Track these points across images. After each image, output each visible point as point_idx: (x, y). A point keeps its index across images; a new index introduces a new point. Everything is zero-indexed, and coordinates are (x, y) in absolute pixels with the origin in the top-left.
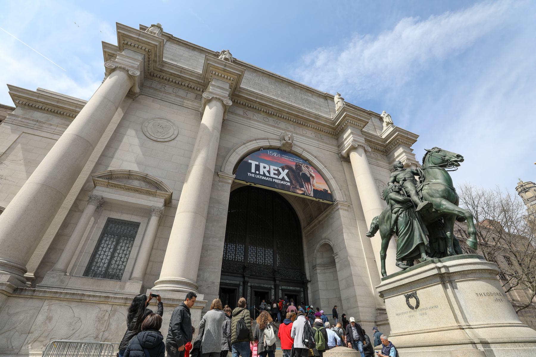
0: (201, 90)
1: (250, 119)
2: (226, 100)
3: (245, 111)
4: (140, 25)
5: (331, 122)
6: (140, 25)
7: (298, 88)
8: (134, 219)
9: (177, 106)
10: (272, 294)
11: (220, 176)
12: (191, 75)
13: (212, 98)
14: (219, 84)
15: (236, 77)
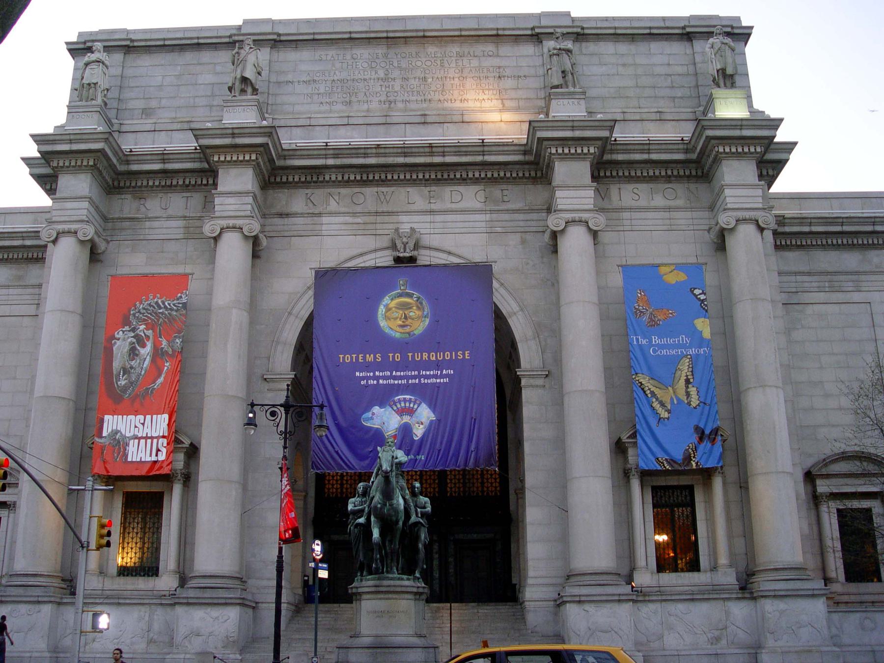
0: (211, 182)
1: (320, 215)
2: (247, 221)
3: (309, 191)
4: (67, 43)
5: (522, 148)
6: (67, 43)
7: (453, 41)
8: (155, 487)
9: (173, 242)
10: (434, 551)
11: (268, 380)
12: (181, 161)
13: (222, 229)
14: (234, 171)
15: (262, 149)
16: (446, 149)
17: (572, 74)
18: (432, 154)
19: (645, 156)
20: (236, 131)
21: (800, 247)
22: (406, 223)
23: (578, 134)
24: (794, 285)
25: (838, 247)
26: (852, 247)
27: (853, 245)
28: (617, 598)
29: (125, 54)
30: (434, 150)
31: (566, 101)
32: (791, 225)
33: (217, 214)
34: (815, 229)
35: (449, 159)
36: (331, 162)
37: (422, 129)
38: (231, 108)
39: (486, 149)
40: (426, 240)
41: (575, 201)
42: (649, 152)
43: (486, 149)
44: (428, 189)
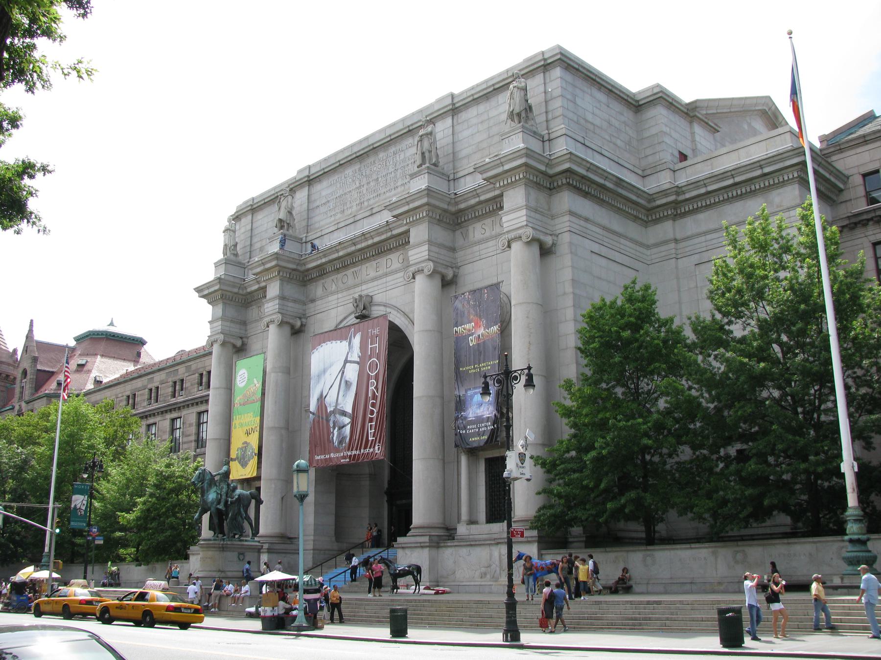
16: (372, 234)
17: (430, 152)
18: (366, 239)
19: (477, 200)
20: (263, 261)
21: (708, 207)
22: (366, 289)
23: (412, 206)
24: (704, 244)
25: (741, 197)
26: (753, 193)
27: (784, 181)
28: (419, 545)
29: (544, 72)
30: (366, 236)
31: (417, 178)
32: (690, 191)
33: (266, 314)
34: (711, 188)
35: (376, 239)
36: (324, 260)
37: (371, 219)
38: (506, 140)
39: (391, 226)
40: (377, 299)
41: (419, 256)
42: (478, 195)
43: (391, 226)
44: (376, 261)
